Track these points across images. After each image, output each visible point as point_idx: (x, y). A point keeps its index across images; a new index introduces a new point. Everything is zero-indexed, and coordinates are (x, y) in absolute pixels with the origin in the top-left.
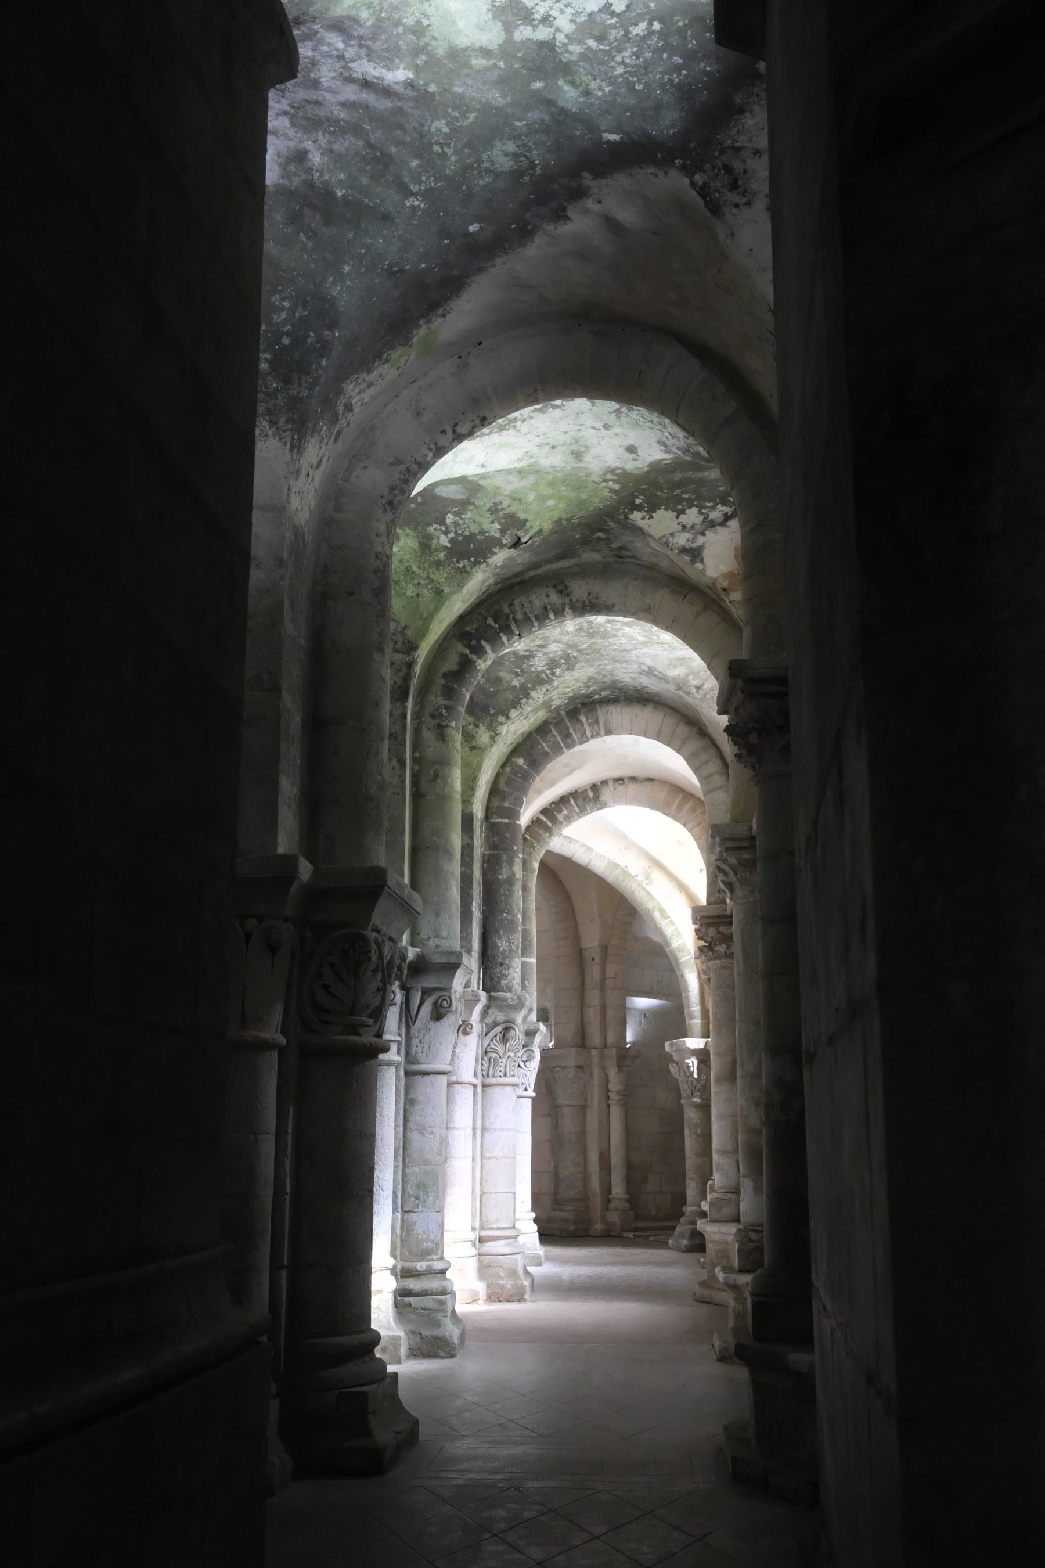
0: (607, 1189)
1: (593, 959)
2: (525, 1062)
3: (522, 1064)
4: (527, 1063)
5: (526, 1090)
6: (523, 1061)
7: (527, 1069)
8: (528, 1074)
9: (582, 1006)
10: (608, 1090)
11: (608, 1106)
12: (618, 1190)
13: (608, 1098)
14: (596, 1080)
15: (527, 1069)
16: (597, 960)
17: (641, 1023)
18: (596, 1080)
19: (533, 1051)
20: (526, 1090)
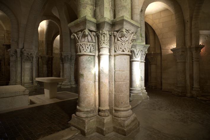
0: (192, 85)
1: (188, 21)
2: (120, 38)
3: (119, 39)
4: (122, 38)
5: (123, 51)
6: (120, 37)
7: (122, 41)
8: (124, 43)
9: (184, 35)
10: (193, 57)
11: (193, 62)
12: (196, 85)
13: (193, 59)
14: (189, 55)
15: (122, 41)
16: (189, 21)
17: (205, 38)
18: (189, 55)
19: (123, 31)
20: (123, 51)
